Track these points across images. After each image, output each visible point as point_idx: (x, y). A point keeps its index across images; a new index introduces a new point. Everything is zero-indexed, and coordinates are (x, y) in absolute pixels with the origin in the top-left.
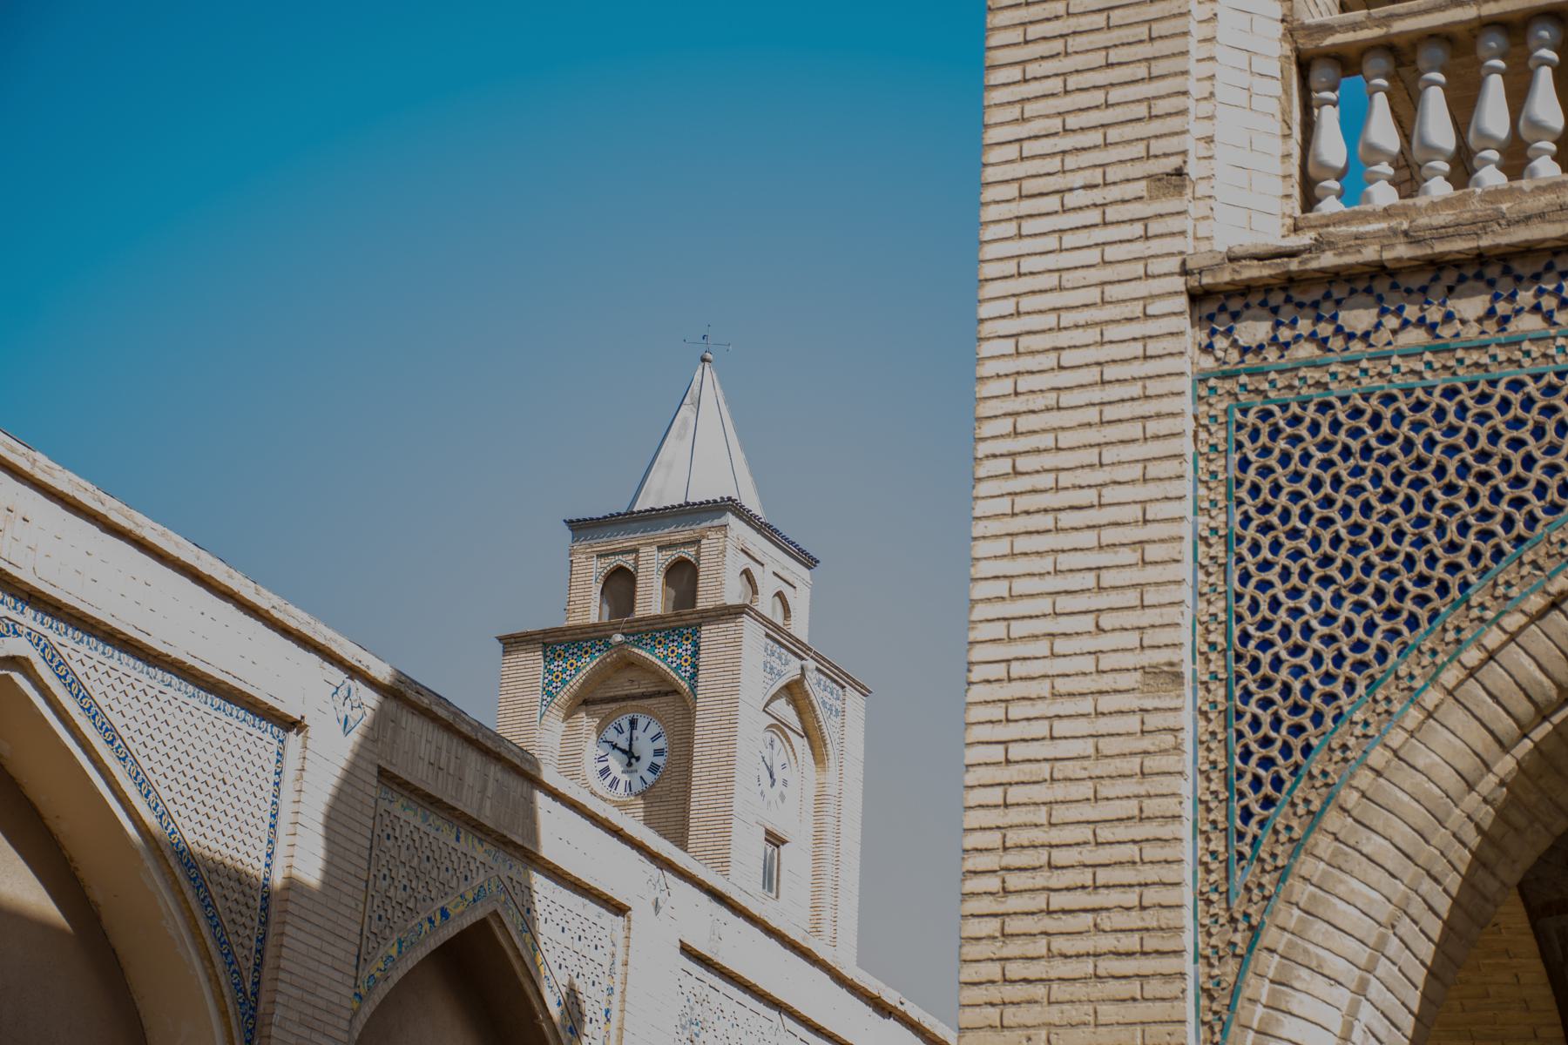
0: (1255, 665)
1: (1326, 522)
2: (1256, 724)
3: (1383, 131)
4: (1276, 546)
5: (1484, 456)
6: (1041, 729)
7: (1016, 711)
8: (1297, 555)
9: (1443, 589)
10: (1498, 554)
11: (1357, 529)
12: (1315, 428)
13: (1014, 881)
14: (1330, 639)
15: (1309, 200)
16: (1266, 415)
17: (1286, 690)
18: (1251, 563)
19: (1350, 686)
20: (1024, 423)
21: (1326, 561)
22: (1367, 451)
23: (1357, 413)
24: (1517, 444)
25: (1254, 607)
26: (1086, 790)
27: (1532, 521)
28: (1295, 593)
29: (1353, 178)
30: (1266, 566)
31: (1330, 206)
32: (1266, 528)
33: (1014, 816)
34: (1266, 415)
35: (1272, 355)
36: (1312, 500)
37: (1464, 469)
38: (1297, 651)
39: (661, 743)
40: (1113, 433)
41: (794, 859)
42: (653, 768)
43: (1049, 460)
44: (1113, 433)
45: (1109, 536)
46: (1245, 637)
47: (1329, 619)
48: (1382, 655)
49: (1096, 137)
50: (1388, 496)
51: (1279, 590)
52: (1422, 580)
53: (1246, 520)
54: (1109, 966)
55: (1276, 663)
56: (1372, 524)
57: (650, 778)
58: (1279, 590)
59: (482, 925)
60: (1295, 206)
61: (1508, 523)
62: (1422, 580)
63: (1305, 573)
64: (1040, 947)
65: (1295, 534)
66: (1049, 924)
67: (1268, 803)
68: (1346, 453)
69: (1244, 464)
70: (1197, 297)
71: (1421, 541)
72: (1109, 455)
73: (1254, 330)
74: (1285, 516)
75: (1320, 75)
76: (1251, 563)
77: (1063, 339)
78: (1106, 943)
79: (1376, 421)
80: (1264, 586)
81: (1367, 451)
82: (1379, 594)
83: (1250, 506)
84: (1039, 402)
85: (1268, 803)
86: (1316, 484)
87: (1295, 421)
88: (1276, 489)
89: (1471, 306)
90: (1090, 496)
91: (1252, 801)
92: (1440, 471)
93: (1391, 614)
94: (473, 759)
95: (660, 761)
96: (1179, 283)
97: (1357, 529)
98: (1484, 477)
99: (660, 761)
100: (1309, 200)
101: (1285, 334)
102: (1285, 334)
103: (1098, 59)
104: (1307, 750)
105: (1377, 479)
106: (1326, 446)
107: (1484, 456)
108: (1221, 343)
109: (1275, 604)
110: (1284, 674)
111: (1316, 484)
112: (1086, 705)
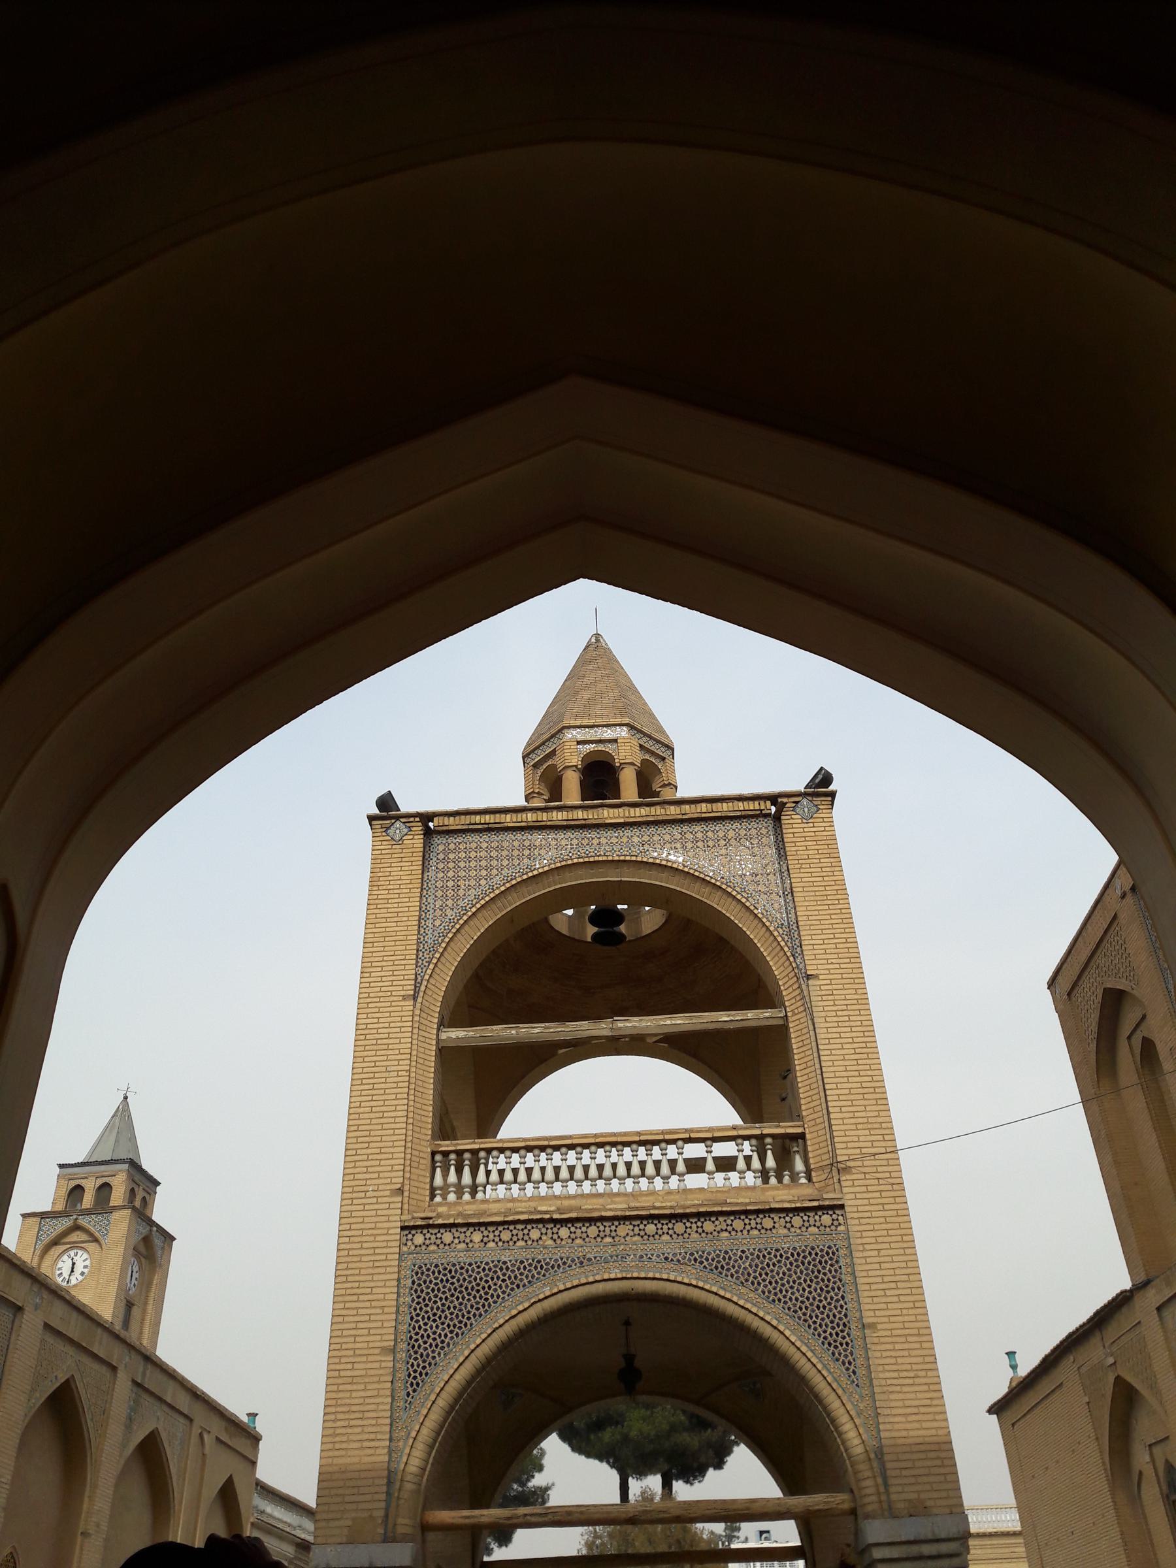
0: (413, 1347)
1: (435, 1302)
2: (412, 1365)
3: (452, 1177)
4: (421, 1309)
5: (478, 1285)
6: (350, 1366)
7: (343, 1360)
8: (427, 1312)
9: (466, 1325)
10: (481, 1315)
11: (452, 1314)
12: (433, 1273)
13: (340, 1416)
14: (434, 1339)
15: (433, 1196)
16: (420, 1267)
17: (422, 1355)
18: (414, 1314)
19: (439, 1354)
20: (350, 1266)
21: (435, 1315)
22: (447, 1281)
23: (445, 1269)
24: (487, 1281)
25: (414, 1328)
26: (362, 1387)
27: (489, 1306)
28: (425, 1324)
29: (445, 1189)
30: (418, 1315)
31: (438, 1199)
32: (418, 1303)
33: (341, 1395)
34: (420, 1267)
35: (424, 1247)
36: (432, 1295)
37: (473, 1288)
38: (425, 1343)
39: (88, 1263)
40: (376, 1271)
41: (135, 1311)
42: (82, 1274)
43: (357, 1278)
44: (376, 1271)
45: (374, 1304)
46: (411, 1338)
47: (434, 1333)
48: (448, 1345)
49: (376, 1175)
50: (452, 1295)
51: (421, 1323)
52: (460, 1322)
53: (413, 1300)
54: (366, 1444)
55: (419, 1346)
56: (447, 1304)
57: (81, 1278)
58: (421, 1323)
59: (67, 1381)
60: (428, 1199)
61: (484, 1306)
62: (460, 1322)
63: (429, 1318)
64: (345, 1438)
65: (427, 1305)
66: (349, 1431)
67: (414, 1391)
68: (442, 1281)
69: (413, 1282)
70: (403, 1228)
71: (460, 1310)
72: (375, 1278)
73: (419, 1239)
74: (424, 1300)
75: (438, 1157)
76: (414, 1314)
77: (364, 1239)
78: (366, 1437)
79: (450, 1271)
80: (417, 1321)
81: (447, 1281)
82: (449, 1326)
83: (414, 1296)
84: (355, 1259)
85: (414, 1391)
86: (433, 1290)
87: (428, 1270)
88: (422, 1291)
89: (477, 1237)
90: (369, 1290)
91: (410, 1389)
92: (467, 1289)
93: (451, 1332)
94: (75, 1314)
95: (86, 1271)
96: (399, 1224)
97: (443, 1305)
98: (478, 1291)
99: (86, 1271)
100: (433, 1196)
101: (428, 1242)
102: (428, 1242)
103: (378, 1151)
104: (426, 1374)
105: (450, 1290)
106: (436, 1278)
107: (478, 1285)
108: (409, 1243)
109: (420, 1327)
110: (421, 1350)
111: (433, 1290)
112: (364, 1359)
